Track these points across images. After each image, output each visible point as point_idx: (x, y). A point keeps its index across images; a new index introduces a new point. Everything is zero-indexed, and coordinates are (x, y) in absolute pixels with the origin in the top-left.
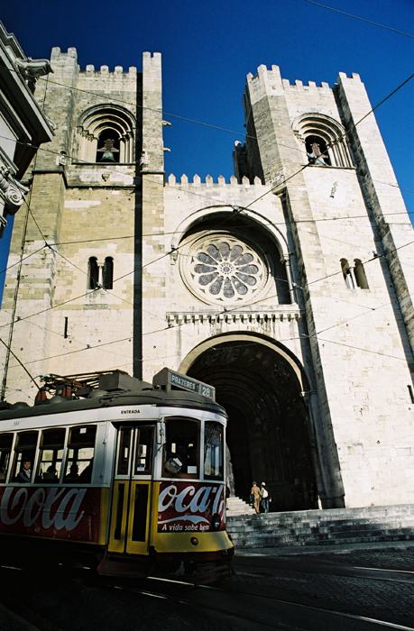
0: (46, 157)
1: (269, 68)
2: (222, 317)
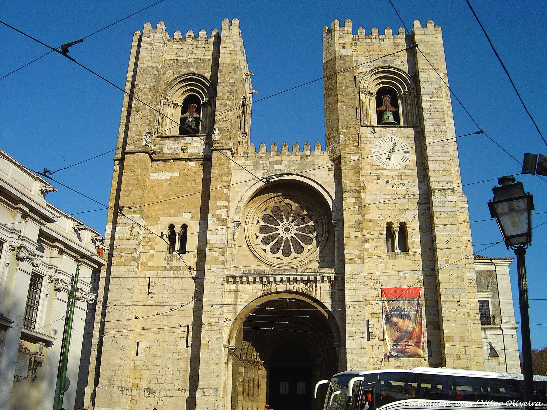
0: (135, 138)
1: (342, 25)
2: (271, 279)
